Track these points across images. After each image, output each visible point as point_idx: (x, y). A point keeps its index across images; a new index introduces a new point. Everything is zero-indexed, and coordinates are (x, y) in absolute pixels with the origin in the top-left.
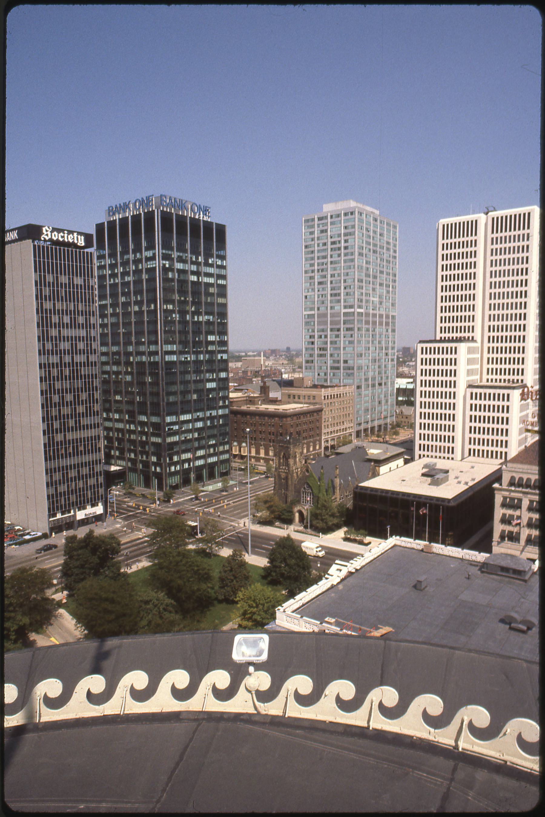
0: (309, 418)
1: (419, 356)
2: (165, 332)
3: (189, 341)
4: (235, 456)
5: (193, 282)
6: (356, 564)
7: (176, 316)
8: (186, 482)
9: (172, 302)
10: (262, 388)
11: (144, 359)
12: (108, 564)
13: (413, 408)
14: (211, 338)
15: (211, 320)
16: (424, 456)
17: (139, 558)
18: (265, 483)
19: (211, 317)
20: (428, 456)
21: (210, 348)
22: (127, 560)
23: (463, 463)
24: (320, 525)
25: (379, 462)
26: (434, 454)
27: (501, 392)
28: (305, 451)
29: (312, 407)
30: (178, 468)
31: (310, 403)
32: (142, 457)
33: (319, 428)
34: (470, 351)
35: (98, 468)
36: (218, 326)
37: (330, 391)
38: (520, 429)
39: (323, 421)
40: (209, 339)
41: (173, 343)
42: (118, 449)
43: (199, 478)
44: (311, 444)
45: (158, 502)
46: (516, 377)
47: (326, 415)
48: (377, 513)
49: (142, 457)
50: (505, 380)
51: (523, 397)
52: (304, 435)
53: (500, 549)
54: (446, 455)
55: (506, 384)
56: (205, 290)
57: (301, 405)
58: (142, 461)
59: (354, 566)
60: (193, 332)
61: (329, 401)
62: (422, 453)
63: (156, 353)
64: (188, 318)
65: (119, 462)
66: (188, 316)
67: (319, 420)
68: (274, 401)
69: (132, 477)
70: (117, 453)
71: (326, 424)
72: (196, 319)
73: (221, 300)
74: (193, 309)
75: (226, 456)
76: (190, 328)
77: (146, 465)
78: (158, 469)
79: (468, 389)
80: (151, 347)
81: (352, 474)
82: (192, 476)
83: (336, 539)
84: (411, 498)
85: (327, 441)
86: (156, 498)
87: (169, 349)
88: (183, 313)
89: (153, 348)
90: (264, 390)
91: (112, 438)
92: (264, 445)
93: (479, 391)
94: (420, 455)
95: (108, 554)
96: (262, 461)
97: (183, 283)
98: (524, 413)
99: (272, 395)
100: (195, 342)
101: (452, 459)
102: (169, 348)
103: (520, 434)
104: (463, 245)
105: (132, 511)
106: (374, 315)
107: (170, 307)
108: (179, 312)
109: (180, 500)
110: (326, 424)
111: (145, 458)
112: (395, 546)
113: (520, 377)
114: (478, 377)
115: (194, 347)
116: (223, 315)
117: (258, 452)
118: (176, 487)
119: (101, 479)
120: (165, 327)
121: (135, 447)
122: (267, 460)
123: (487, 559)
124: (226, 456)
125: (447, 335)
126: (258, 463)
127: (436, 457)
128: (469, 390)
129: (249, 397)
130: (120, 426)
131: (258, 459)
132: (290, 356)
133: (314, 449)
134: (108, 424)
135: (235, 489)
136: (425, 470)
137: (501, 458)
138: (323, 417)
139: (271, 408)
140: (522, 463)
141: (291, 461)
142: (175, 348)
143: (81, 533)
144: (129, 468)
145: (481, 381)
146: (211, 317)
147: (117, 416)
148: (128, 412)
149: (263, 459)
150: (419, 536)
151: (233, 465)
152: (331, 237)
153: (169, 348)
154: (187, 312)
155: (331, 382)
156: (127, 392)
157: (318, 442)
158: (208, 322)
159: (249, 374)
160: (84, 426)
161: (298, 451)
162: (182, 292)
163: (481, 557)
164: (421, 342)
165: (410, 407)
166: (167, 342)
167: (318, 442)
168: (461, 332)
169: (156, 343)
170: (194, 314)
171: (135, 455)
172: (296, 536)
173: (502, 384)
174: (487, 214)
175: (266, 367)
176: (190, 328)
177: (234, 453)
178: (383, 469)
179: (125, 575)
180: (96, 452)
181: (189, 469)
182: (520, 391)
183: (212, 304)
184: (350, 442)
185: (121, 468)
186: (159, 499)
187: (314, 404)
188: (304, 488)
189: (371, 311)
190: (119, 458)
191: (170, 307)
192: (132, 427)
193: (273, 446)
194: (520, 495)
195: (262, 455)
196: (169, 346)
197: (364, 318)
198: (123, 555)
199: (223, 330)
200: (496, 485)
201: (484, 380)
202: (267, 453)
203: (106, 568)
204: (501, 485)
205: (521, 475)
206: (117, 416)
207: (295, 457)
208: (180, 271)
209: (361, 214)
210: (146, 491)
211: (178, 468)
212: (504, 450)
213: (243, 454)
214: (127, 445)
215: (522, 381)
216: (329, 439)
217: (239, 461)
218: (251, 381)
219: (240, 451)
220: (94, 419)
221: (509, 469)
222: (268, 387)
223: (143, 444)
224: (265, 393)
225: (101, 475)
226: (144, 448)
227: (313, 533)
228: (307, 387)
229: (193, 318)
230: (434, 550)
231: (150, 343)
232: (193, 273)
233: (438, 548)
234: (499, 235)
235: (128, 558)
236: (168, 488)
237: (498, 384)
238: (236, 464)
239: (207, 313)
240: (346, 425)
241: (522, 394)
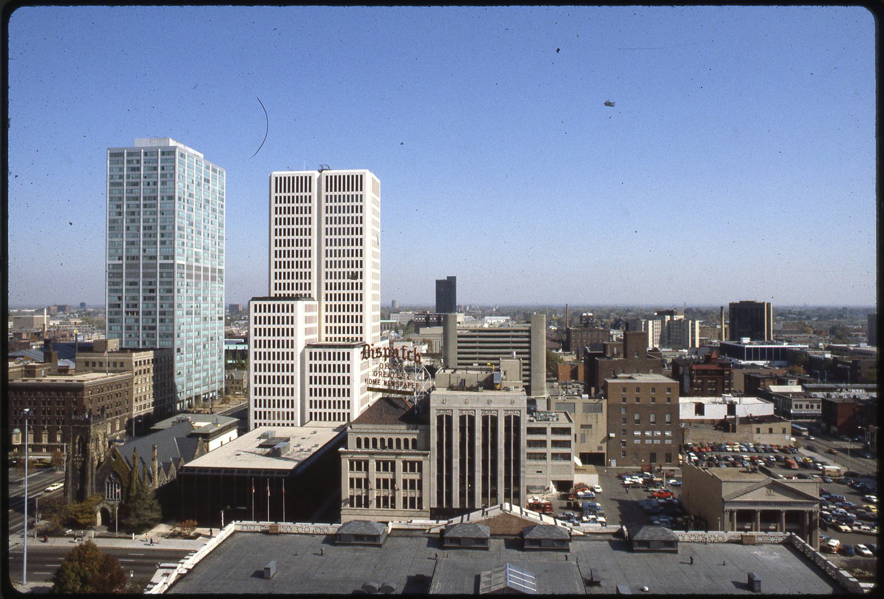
1: (253, 314)
6: (190, 562)
13: (245, 372)
20: (265, 424)
23: (303, 429)
24: (126, 521)
25: (207, 437)
26: (272, 422)
27: (342, 350)
28: (109, 432)
33: (130, 402)
34: (308, 309)
38: (362, 389)
46: (355, 335)
48: (206, 497)
51: (365, 355)
52: (108, 411)
53: (348, 515)
54: (286, 422)
55: (346, 343)
59: (185, 566)
62: (258, 421)
83: (157, 537)
84: (249, 474)
93: (318, 350)
94: (256, 424)
96: (44, 450)
101: (293, 425)
103: (362, 394)
104: (297, 199)
106: (198, 268)
112: (235, 532)
113: (359, 336)
114: (316, 336)
117: (37, 438)
123: (339, 529)
125: (282, 292)
127: (274, 425)
128: (308, 351)
129: (26, 366)
132: (86, 315)
136: (262, 441)
137: (344, 420)
139: (61, 379)
140: (367, 423)
141: (92, 446)
145: (320, 340)
150: (260, 517)
152: (145, 177)
155: (144, 343)
159: (24, 336)
161: (100, 432)
163: (332, 528)
164: (254, 299)
165: (242, 372)
172: (101, 543)
173: (342, 343)
174: (320, 171)
175: (51, 327)
178: (213, 444)
182: (361, 349)
188: (110, 479)
189: (194, 264)
194: (392, 458)
195: (45, 441)
197: (185, 271)
200: (341, 449)
201: (323, 339)
202: (52, 438)
204: (346, 448)
205: (390, 436)
207: (97, 439)
209: (182, 155)
212: (346, 411)
215: (361, 339)
218: (27, 346)
227: (124, 535)
230: (281, 530)
233: (285, 526)
234: (333, 193)
237: (337, 343)
241: (364, 352)
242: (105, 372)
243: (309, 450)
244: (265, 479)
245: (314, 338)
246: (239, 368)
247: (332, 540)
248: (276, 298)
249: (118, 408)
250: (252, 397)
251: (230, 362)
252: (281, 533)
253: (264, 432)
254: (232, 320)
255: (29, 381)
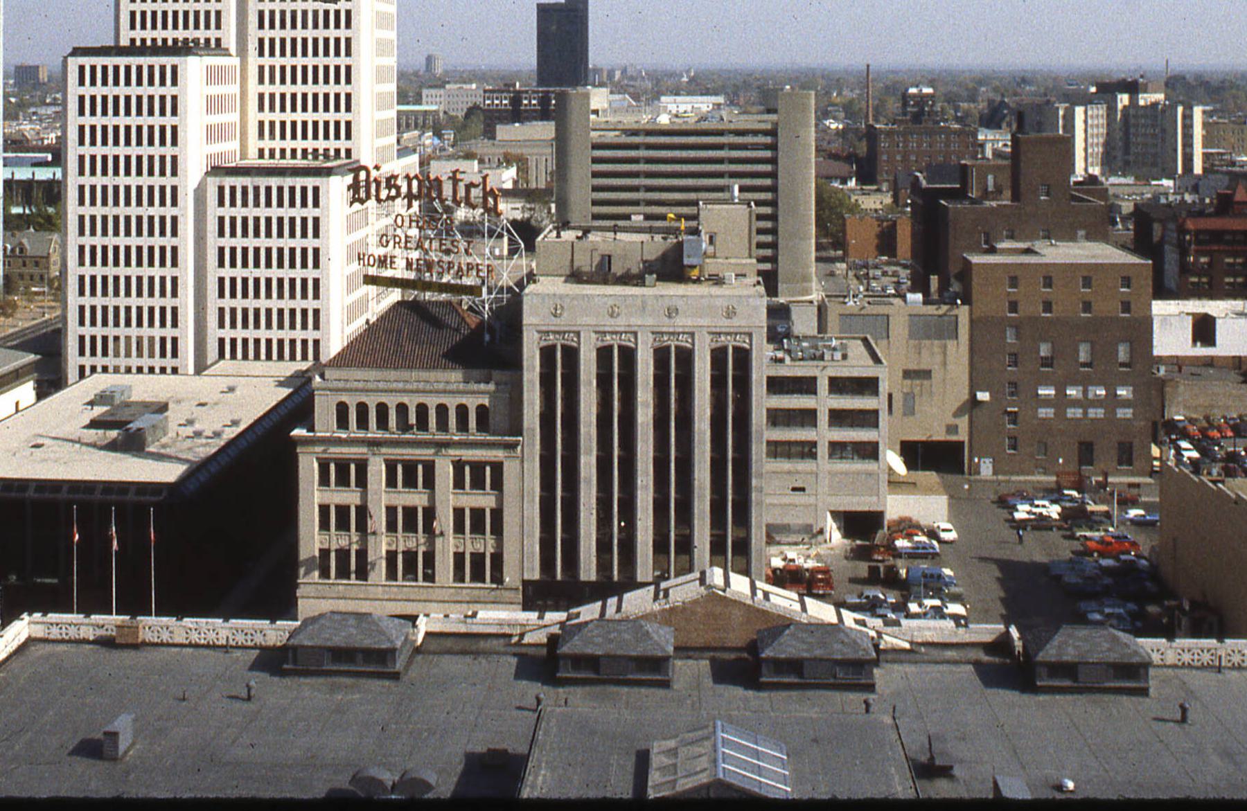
1: (74, 90)
13: (55, 237)
16: (93, 369)
20: (105, 369)
23: (203, 382)
26: (122, 362)
27: (299, 182)
34: (214, 76)
38: (350, 279)
46: (332, 144)
50: (305, 151)
51: (358, 193)
53: (317, 598)
54: (157, 362)
55: (309, 162)
62: (87, 361)
79: (210, 180)
84: (63, 495)
93: (239, 182)
94: (82, 368)
98: (358, 235)
101: (175, 371)
103: (350, 290)
113: (342, 144)
114: (233, 146)
125: (149, 34)
127: (128, 370)
128: (213, 184)
136: (99, 410)
137: (305, 357)
140: (362, 365)
163: (274, 632)
164: (77, 52)
168: (186, 27)
173: (299, 162)
182: (349, 179)
200: (298, 432)
201: (253, 152)
212: (311, 335)
215: (348, 152)
221: (330, 385)
230: (146, 635)
233: (154, 626)
237: (288, 162)
241: (354, 187)
243: (217, 434)
244: (104, 508)
245: (229, 149)
246: (39, 227)
247: (274, 661)
248: (133, 49)
250: (73, 300)
251: (16, 210)
252: (145, 644)
253: (101, 388)
254: (22, 105)
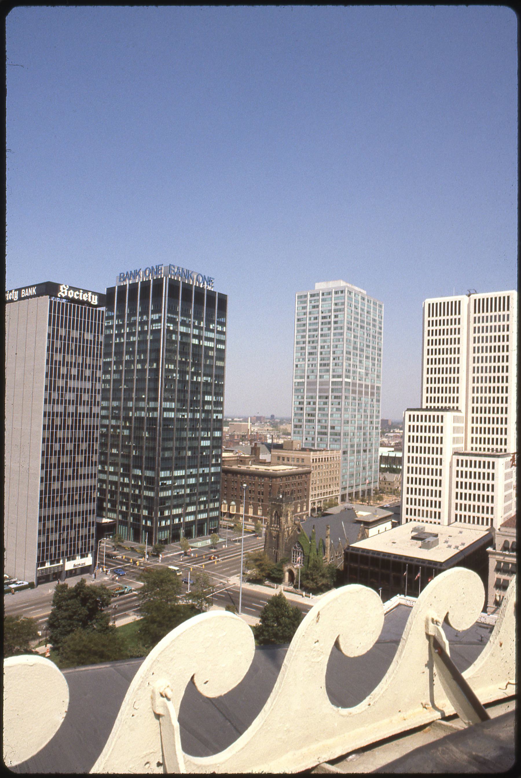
0: (297, 480)
2: (166, 390)
3: (187, 400)
4: (225, 513)
5: (194, 345)
7: (176, 376)
8: (176, 537)
9: (173, 362)
10: (252, 449)
11: (143, 414)
12: (97, 616)
14: (208, 398)
15: (209, 381)
16: (411, 520)
17: (127, 612)
18: (253, 542)
19: (209, 378)
21: (206, 407)
22: (115, 613)
27: (487, 459)
29: (300, 469)
30: (168, 523)
31: (299, 466)
32: (133, 510)
33: (307, 490)
34: (456, 420)
35: (91, 518)
36: (215, 388)
37: (318, 455)
39: (311, 483)
40: (206, 399)
41: (172, 400)
42: (110, 501)
43: (188, 534)
44: (299, 505)
45: (147, 556)
46: (499, 447)
47: (313, 478)
49: (133, 510)
50: (489, 449)
54: (433, 520)
55: (490, 452)
56: (205, 352)
57: (291, 467)
58: (133, 515)
60: (192, 392)
61: (318, 464)
62: (409, 517)
63: (155, 409)
64: (187, 378)
65: (110, 515)
66: (187, 376)
67: (307, 482)
68: (264, 463)
69: (122, 530)
70: (109, 506)
71: (314, 486)
72: (195, 380)
73: (219, 363)
74: (193, 370)
75: (215, 514)
76: (189, 388)
77: (137, 518)
78: (149, 523)
79: (454, 456)
80: (150, 403)
81: (343, 537)
82: (182, 531)
85: (314, 503)
86: (146, 551)
87: (168, 407)
88: (183, 373)
89: (152, 404)
90: (255, 451)
91: (105, 490)
92: (253, 504)
93: (465, 458)
94: (407, 519)
95: (97, 605)
96: (250, 520)
97: (184, 345)
98: (509, 481)
99: (262, 457)
100: (192, 401)
101: (439, 523)
102: (167, 405)
105: (120, 564)
107: (172, 367)
108: (180, 372)
109: (169, 555)
110: (314, 486)
111: (136, 510)
113: (503, 447)
114: (463, 445)
115: (191, 406)
116: (220, 376)
117: (246, 511)
118: (166, 542)
119: (93, 530)
120: (165, 386)
121: (127, 499)
122: (255, 519)
124: (215, 514)
125: (433, 405)
126: (246, 522)
128: (456, 457)
129: (240, 457)
130: (115, 478)
131: (247, 518)
133: (302, 510)
134: (103, 476)
135: (224, 546)
137: (487, 524)
138: (311, 479)
139: (262, 468)
142: (173, 405)
143: (72, 583)
144: (119, 520)
145: (466, 449)
146: (209, 378)
147: (112, 469)
148: (123, 465)
149: (251, 518)
151: (222, 522)
152: (322, 312)
153: (167, 405)
154: (187, 373)
156: (124, 446)
157: (305, 504)
158: (206, 383)
160: (81, 475)
162: (184, 353)
164: (408, 410)
166: (166, 400)
167: (305, 504)
168: (446, 402)
169: (155, 400)
170: (193, 374)
171: (127, 509)
174: (469, 296)
176: (189, 388)
177: (223, 511)
178: (372, 531)
179: (113, 629)
180: (90, 502)
181: (180, 525)
183: (211, 366)
184: (336, 505)
185: (111, 520)
186: (148, 553)
187: (303, 466)
190: (110, 510)
191: (172, 367)
192: (126, 480)
193: (262, 505)
195: (251, 514)
196: (168, 403)
198: (111, 608)
199: (219, 391)
202: (255, 512)
203: (94, 621)
206: (112, 469)
208: (182, 334)
209: (350, 293)
210: (135, 545)
211: (168, 523)
213: (231, 512)
214: (119, 498)
215: (505, 450)
216: (316, 501)
217: (228, 519)
219: (229, 509)
220: (92, 469)
222: (259, 448)
223: (136, 497)
224: (255, 454)
225: (93, 526)
226: (137, 501)
228: (296, 450)
229: (192, 378)
231: (150, 400)
232: (195, 337)
234: (481, 315)
235: (116, 611)
236: (157, 543)
238: (224, 522)
239: (205, 375)
240: (333, 488)
242: (291, 465)
245: (460, 447)
248: (427, 409)
249: (300, 494)
250: (405, 495)
253: (414, 526)
255: (242, 468)
